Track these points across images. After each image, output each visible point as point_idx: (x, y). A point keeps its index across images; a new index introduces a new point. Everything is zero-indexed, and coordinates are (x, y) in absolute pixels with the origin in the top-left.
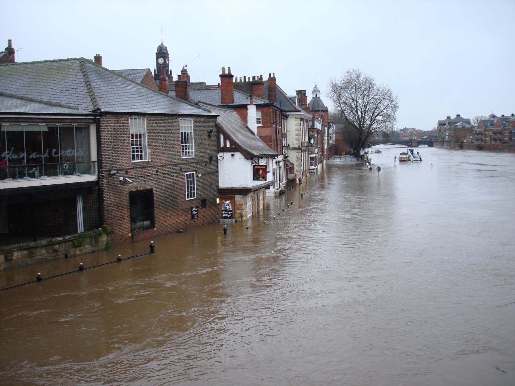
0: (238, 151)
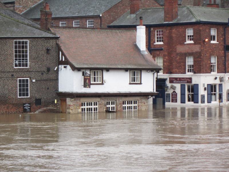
0: (67, 64)
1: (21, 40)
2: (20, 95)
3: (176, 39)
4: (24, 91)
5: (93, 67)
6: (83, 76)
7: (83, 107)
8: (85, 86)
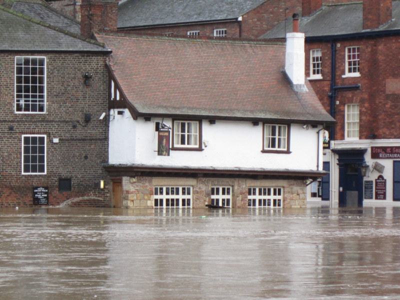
0: (125, 107)
1: (31, 57)
2: (26, 170)
3: (385, 65)
4: (34, 160)
5: (178, 112)
6: (157, 132)
7: (159, 197)
8: (160, 152)
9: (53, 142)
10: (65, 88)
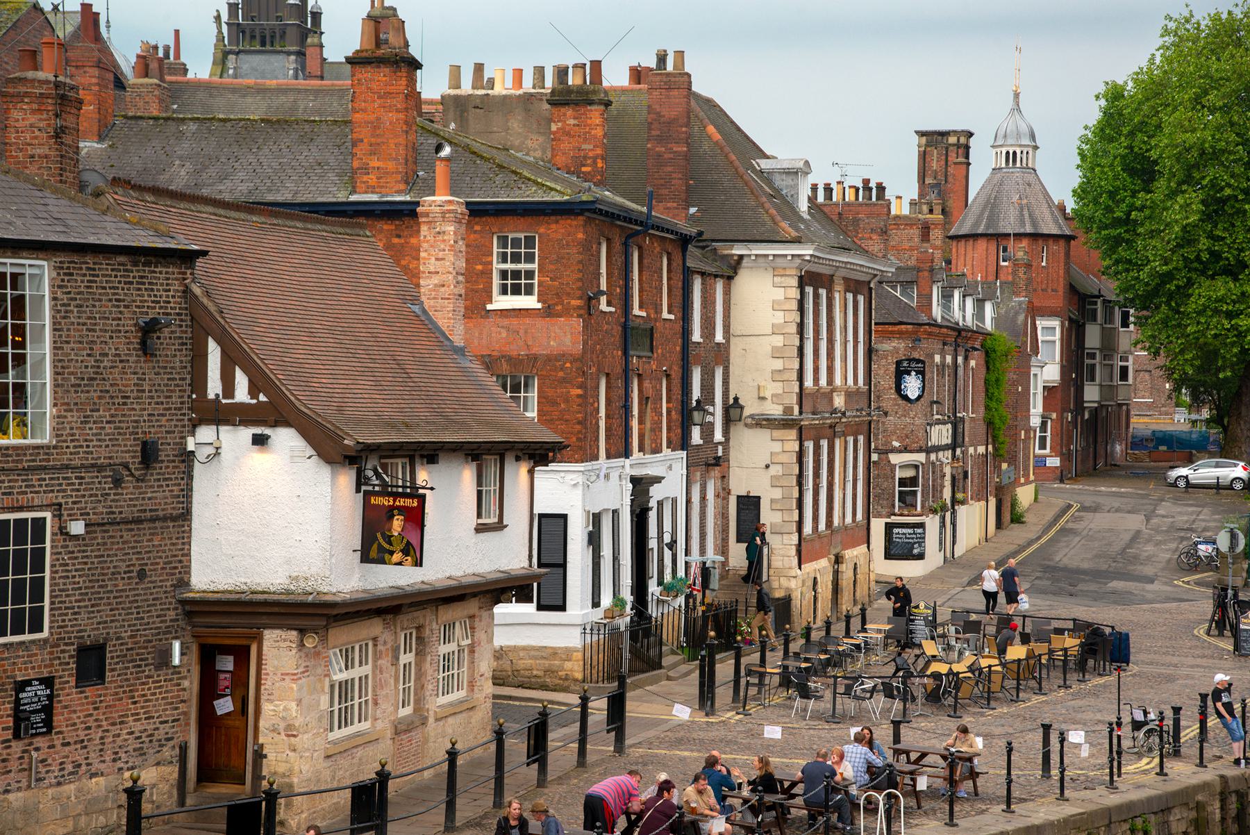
8: (373, 553)
9: (67, 534)
10: (96, 361)
